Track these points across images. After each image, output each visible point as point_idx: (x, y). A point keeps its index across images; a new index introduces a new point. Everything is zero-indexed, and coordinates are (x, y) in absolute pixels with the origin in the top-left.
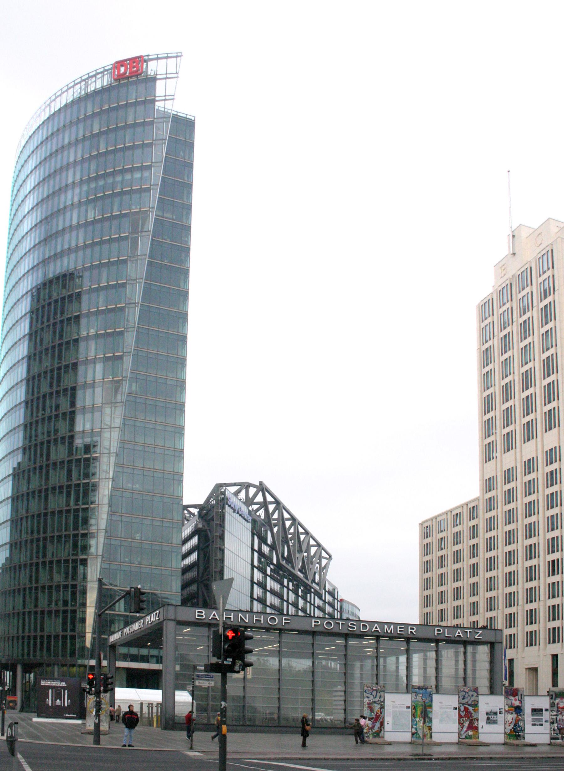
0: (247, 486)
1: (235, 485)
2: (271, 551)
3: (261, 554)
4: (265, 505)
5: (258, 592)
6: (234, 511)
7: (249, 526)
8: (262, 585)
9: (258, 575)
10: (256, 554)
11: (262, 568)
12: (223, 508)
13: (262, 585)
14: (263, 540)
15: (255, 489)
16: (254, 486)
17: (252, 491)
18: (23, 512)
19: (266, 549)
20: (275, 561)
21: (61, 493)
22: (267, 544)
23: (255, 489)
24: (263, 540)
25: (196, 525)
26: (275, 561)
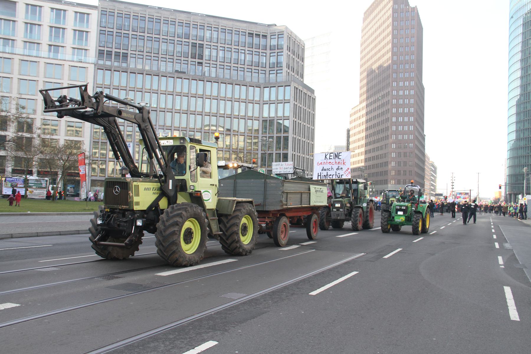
18: (522, 136)
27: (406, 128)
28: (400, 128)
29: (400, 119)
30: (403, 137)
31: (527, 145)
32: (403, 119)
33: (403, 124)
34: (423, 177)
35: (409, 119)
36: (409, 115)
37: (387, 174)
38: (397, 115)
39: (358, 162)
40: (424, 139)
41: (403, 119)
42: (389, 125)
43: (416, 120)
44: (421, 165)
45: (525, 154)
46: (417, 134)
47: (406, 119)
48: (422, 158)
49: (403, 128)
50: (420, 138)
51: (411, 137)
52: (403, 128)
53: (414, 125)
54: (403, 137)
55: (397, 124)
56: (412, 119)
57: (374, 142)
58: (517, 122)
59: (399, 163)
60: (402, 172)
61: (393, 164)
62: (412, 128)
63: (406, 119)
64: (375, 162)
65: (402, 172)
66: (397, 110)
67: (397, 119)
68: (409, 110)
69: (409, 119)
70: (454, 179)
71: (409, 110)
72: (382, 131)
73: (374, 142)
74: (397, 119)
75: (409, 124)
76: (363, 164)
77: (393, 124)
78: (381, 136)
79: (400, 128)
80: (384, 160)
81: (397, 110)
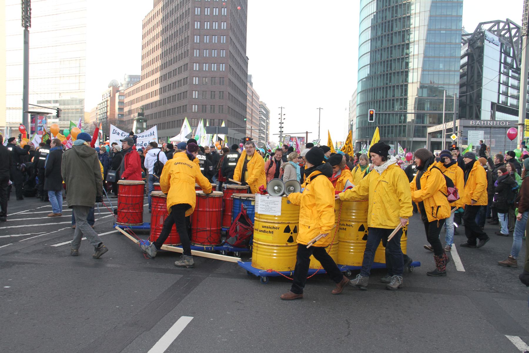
0: (498, 22)
1: (491, 22)
2: (512, 61)
3: (505, 63)
4: (509, 30)
5: (503, 88)
6: (490, 42)
7: (499, 48)
8: (506, 84)
9: (503, 78)
10: (502, 65)
11: (506, 73)
12: (483, 42)
13: (506, 84)
14: (507, 54)
15: (503, 24)
16: (503, 22)
17: (502, 25)
18: (379, 59)
19: (509, 60)
20: (515, 67)
21: (399, 48)
22: (509, 56)
23: (503, 24)
24: (507, 54)
25: (467, 50)
26: (515, 67)
27: (215, 39)
28: (207, 39)
29: (207, 25)
30: (210, 54)
31: (386, 72)
32: (211, 26)
33: (211, 33)
34: (242, 117)
35: (220, 26)
36: (220, 19)
37: (186, 111)
38: (202, 19)
39: (152, 94)
40: (246, 64)
41: (211, 26)
42: (189, 34)
43: (230, 28)
44: (240, 99)
45: (382, 84)
46: (231, 48)
47: (215, 26)
48: (242, 89)
49: (211, 40)
50: (239, 60)
51: (223, 53)
52: (211, 40)
53: (227, 36)
54: (210, 54)
55: (201, 32)
56: (224, 26)
57: (171, 63)
58: (373, 40)
59: (203, 93)
60: (208, 107)
61: (195, 95)
62: (224, 39)
63: (215, 26)
64: (172, 93)
65: (208, 107)
66: (202, 11)
67: (202, 25)
68: (220, 11)
69: (220, 26)
70: (283, 117)
71: (220, 11)
72: (181, 44)
73: (171, 63)
74: (202, 25)
75: (220, 33)
76: (157, 98)
77: (195, 32)
78: (179, 52)
79: (207, 39)
80: (183, 89)
81: (202, 11)
